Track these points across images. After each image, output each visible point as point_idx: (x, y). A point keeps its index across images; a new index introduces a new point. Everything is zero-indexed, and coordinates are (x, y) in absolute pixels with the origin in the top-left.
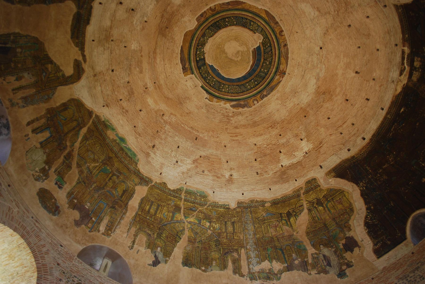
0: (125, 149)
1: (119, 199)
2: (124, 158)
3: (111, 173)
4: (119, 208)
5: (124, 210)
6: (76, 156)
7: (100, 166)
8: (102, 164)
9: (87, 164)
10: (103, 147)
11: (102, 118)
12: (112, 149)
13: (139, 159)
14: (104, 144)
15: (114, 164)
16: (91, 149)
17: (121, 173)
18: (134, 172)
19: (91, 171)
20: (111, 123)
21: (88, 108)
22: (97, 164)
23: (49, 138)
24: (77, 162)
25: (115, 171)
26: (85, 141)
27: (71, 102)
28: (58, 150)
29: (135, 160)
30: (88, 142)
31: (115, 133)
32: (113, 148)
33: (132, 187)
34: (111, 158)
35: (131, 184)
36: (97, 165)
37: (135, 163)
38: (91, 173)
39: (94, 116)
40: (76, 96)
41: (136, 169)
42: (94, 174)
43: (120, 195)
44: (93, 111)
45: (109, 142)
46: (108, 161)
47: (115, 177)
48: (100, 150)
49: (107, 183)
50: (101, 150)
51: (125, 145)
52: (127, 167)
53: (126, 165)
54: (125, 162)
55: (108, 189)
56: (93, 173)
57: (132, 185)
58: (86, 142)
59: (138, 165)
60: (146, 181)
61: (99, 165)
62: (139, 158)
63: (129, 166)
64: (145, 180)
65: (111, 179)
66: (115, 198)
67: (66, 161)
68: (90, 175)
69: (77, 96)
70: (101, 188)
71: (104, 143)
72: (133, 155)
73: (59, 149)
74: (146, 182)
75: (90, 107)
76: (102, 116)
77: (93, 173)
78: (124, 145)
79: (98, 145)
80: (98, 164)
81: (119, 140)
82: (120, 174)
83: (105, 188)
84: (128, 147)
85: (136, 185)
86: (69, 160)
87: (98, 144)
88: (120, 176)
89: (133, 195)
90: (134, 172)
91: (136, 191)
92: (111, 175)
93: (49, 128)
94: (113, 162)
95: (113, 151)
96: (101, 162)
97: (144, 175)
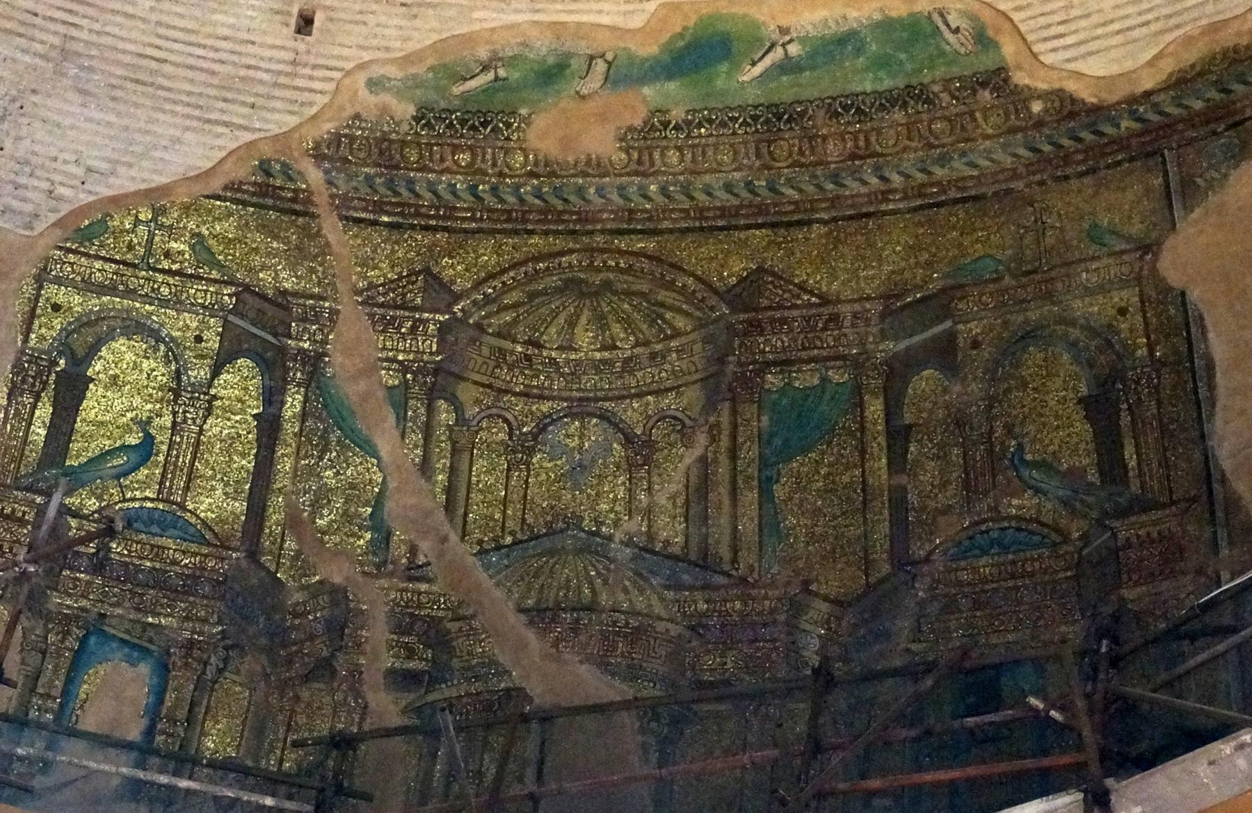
0: (786, 90)
1: (1106, 514)
2: (853, 157)
3: (858, 390)
4: (1165, 585)
5: (1225, 552)
6: (483, 576)
7: (725, 442)
8: (725, 408)
9: (619, 536)
10: (607, 284)
11: (384, 110)
12: (701, 212)
13: (987, 16)
14: (602, 251)
15: (825, 300)
16: (545, 407)
17: (943, 291)
18: (1044, 161)
19: (693, 556)
20: (483, 53)
21: (216, 185)
22: (690, 457)
23: (160, 700)
24: (521, 610)
25: (883, 336)
26: (445, 415)
27: (56, 308)
28: (305, 694)
29: (956, 70)
30: (467, 393)
31: (594, 83)
32: (701, 197)
33: (1129, 297)
34: (754, 280)
35: (1103, 289)
36: (703, 460)
37: (984, 85)
38: (704, 561)
39: (314, 176)
40: (40, 227)
41: (1039, 124)
42: (735, 550)
43: (1093, 476)
44: (267, 151)
45: (621, 189)
46: (756, 327)
47: (925, 381)
48: (617, 329)
49: (898, 502)
50: (627, 323)
51: (767, 61)
52: (953, 194)
53: (920, 191)
54: (896, 179)
55: (950, 528)
56: (725, 552)
57: (1124, 283)
58: (458, 408)
59: (1020, 78)
60: (1211, 116)
61: (714, 439)
62: (973, 18)
63: (959, 167)
64: (1191, 120)
65: (910, 427)
66: (1066, 539)
67: (431, 698)
68: (706, 587)
69: (53, 218)
70: (881, 581)
71: (591, 251)
72: (903, 56)
73: (307, 678)
74: (1215, 133)
75: (224, 154)
76: (369, 102)
77: (725, 552)
78: (758, 69)
79: (561, 320)
80: (702, 439)
81: (672, 86)
82: (946, 312)
83: (918, 550)
84: (803, 40)
85: (1148, 248)
86: (455, 663)
87: (555, 314)
88: (961, 327)
89: (1199, 348)
90: (1044, 161)
91: (1194, 295)
92: (875, 408)
93: (92, 640)
94: (802, 287)
95: (723, 211)
96: (710, 406)
97: (1148, 94)
